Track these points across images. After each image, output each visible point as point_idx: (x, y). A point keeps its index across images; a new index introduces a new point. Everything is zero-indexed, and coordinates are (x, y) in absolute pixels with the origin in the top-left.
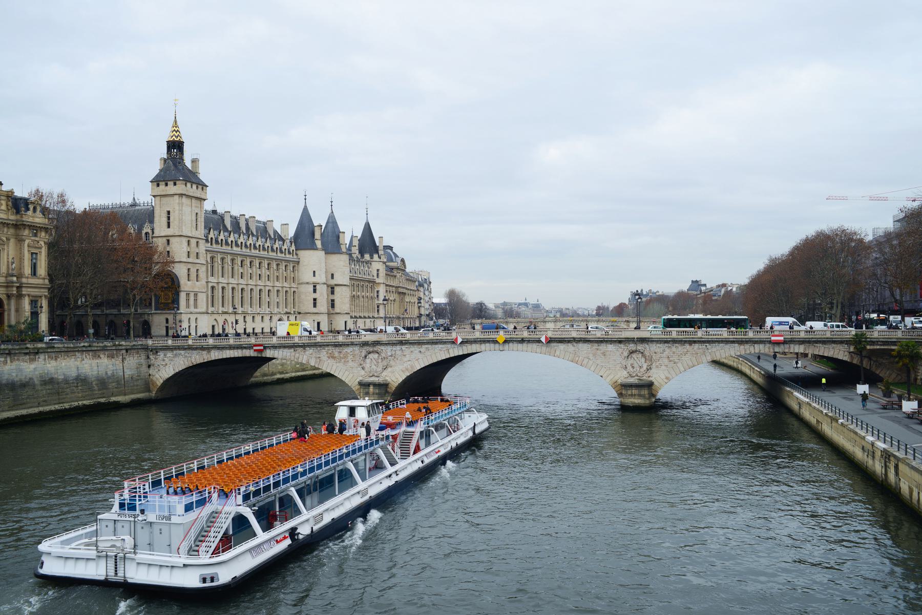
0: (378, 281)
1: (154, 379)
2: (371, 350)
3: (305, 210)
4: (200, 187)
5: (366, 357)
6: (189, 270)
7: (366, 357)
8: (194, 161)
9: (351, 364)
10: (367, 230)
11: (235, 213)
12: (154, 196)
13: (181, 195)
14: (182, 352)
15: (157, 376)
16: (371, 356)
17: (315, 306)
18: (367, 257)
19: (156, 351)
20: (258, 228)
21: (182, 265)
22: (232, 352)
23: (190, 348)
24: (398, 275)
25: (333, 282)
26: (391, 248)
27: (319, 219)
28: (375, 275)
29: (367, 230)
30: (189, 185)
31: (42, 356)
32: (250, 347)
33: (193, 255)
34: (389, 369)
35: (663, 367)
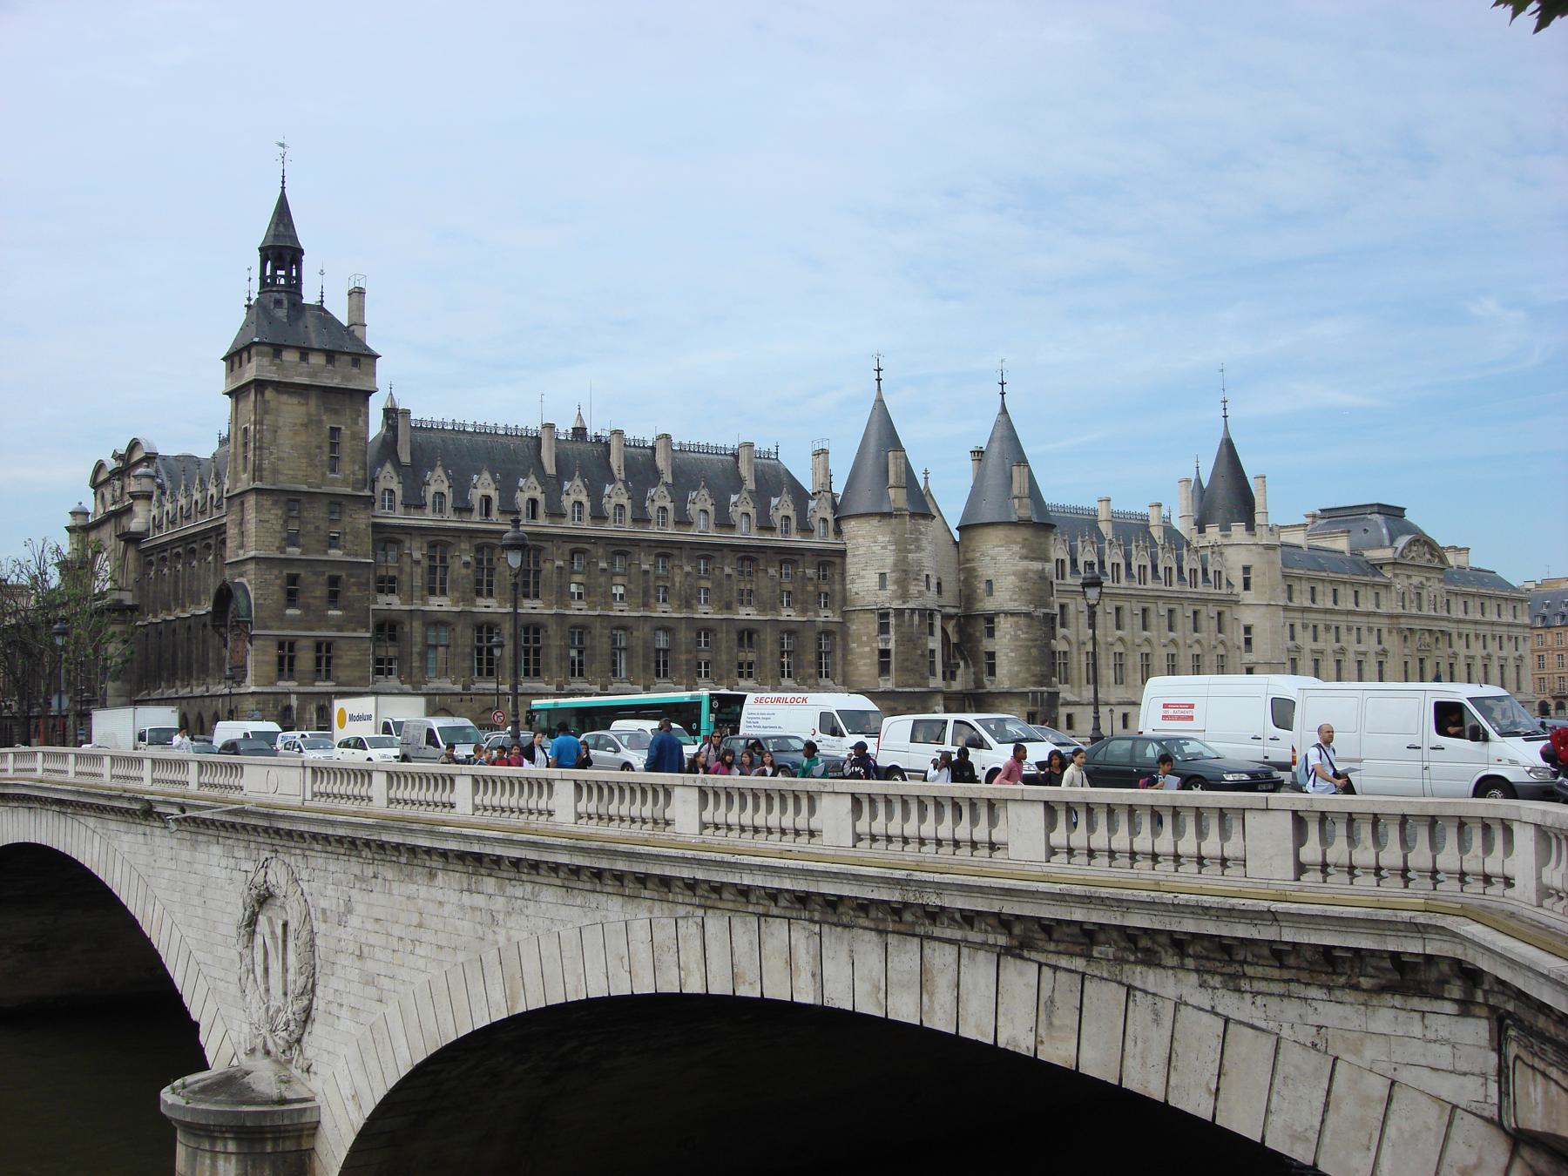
8: (357, 294)
10: (1229, 455)
11: (642, 431)
17: (884, 669)
18: (1213, 533)
20: (629, 464)
24: (1399, 584)
26: (1393, 513)
28: (1238, 581)
29: (1229, 455)
30: (290, 356)
35: (346, 1023)
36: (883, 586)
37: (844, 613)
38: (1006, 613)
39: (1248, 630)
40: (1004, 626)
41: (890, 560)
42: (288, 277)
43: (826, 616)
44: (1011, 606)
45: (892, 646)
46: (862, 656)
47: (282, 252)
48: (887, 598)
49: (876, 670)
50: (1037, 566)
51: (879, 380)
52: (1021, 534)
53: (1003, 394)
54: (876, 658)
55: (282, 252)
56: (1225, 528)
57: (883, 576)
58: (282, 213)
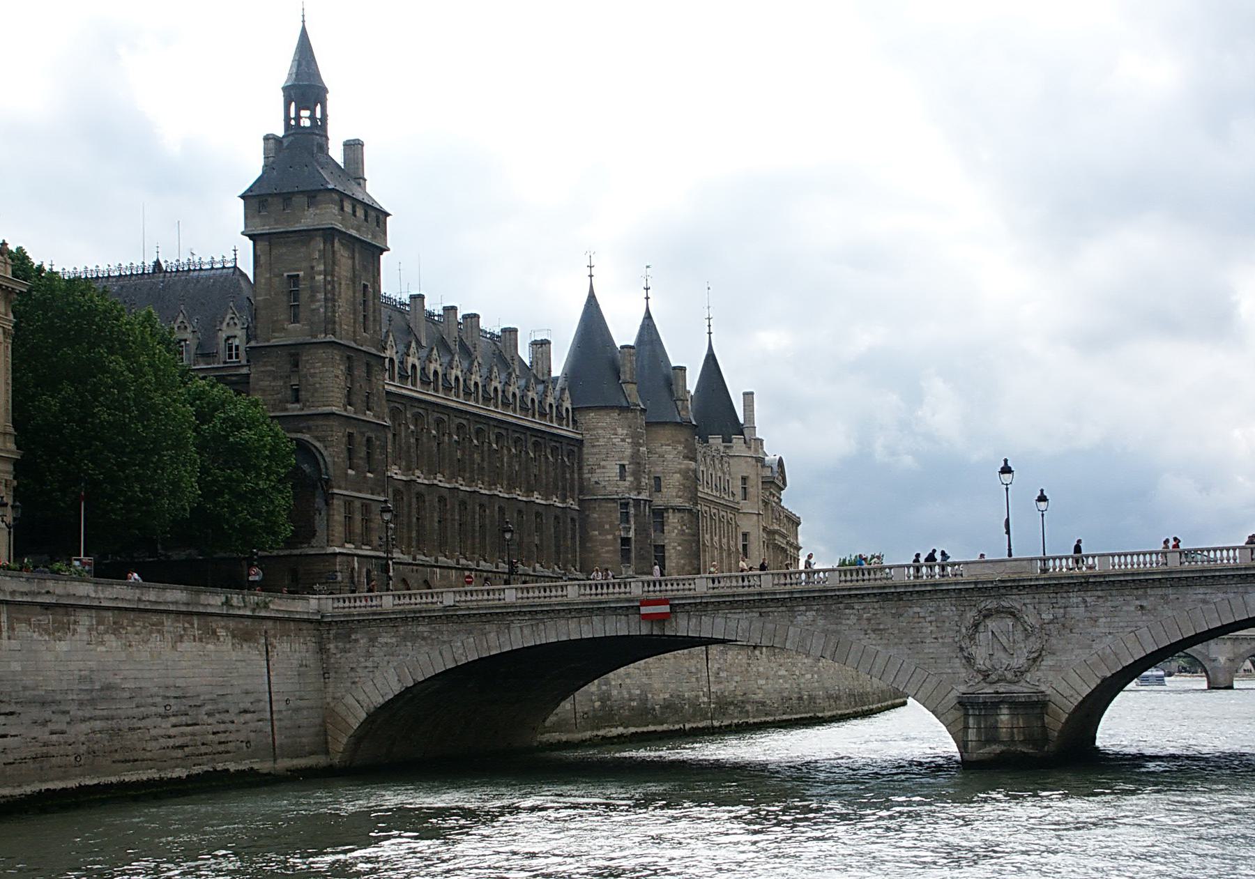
0: (746, 507)
1: (341, 709)
2: (991, 604)
3: (592, 305)
4: (373, 214)
5: (976, 626)
6: (350, 435)
7: (976, 626)
8: (354, 148)
9: (930, 648)
12: (251, 237)
13: (330, 234)
14: (423, 629)
15: (350, 700)
16: (991, 624)
19: (345, 627)
21: (334, 423)
22: (573, 624)
23: (450, 616)
25: (659, 501)
27: (623, 332)
28: (739, 491)
31: (84, 619)
32: (630, 609)
33: (358, 399)
34: (1048, 661)
36: (622, 477)
37: (581, 502)
38: (676, 509)
39: (745, 535)
40: (673, 519)
41: (628, 452)
42: (312, 118)
43: (572, 503)
44: (677, 502)
45: (632, 534)
46: (605, 543)
47: (305, 89)
48: (624, 489)
49: (618, 558)
50: (693, 465)
51: (591, 276)
52: (683, 435)
53: (647, 298)
54: (619, 546)
55: (305, 89)
56: (727, 440)
57: (623, 466)
58: (305, 51)
